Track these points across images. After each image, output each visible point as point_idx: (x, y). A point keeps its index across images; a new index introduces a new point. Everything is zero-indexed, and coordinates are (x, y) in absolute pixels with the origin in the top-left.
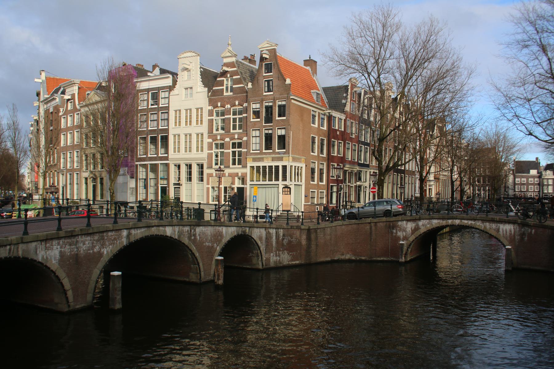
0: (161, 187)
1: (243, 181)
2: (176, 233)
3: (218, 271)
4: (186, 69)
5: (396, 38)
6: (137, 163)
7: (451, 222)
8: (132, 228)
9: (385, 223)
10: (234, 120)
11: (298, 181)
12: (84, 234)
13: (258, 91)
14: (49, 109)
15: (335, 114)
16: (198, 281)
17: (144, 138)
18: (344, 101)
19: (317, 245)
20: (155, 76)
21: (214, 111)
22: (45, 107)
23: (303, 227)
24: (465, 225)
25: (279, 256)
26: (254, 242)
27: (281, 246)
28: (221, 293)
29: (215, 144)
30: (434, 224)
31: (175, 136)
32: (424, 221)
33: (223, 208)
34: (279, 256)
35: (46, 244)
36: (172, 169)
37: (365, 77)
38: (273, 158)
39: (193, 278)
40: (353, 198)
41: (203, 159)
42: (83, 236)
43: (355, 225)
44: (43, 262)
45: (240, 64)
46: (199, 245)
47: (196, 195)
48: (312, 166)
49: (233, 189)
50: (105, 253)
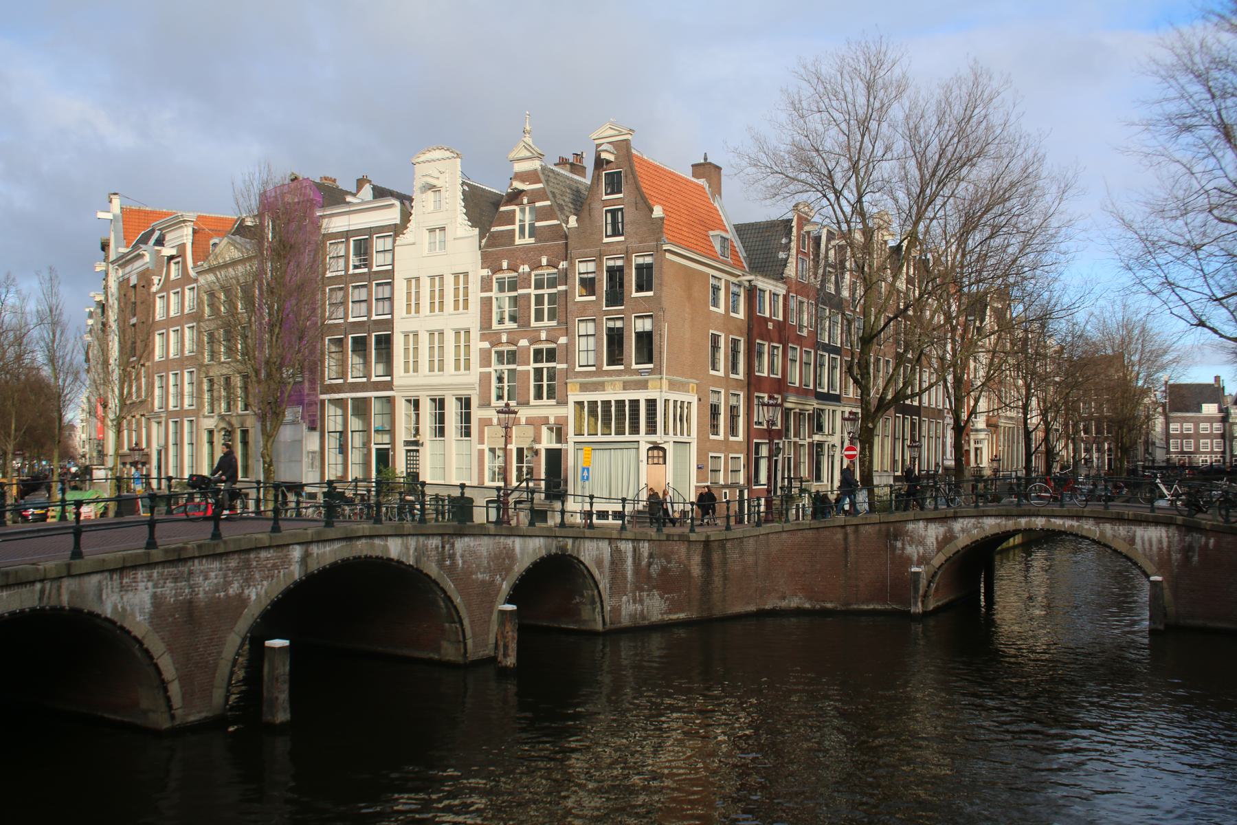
0: (377, 449)
1: (560, 434)
2: (411, 552)
3: (504, 637)
4: (432, 187)
5: (897, 112)
6: (323, 397)
7: (1026, 523)
8: (311, 542)
9: (877, 527)
10: (539, 299)
11: (682, 434)
12: (207, 556)
13: (592, 234)
14: (128, 280)
15: (762, 283)
16: (460, 659)
17: (340, 342)
18: (782, 255)
19: (725, 578)
20: (363, 202)
21: (494, 280)
22: (120, 273)
23: (693, 537)
24: (1057, 529)
25: (641, 602)
26: (586, 572)
27: (644, 580)
28: (512, 688)
29: (496, 352)
30: (987, 527)
31: (406, 336)
32: (966, 521)
33: (516, 495)
34: (641, 602)
35: (121, 578)
36: (402, 409)
37: (828, 200)
38: (624, 382)
39: (449, 652)
40: (804, 472)
41: (469, 386)
42: (204, 561)
43: (810, 532)
44: (116, 619)
45: (551, 175)
46: (463, 579)
47: (454, 466)
48: (713, 399)
49: (536, 453)
50: (253, 597)
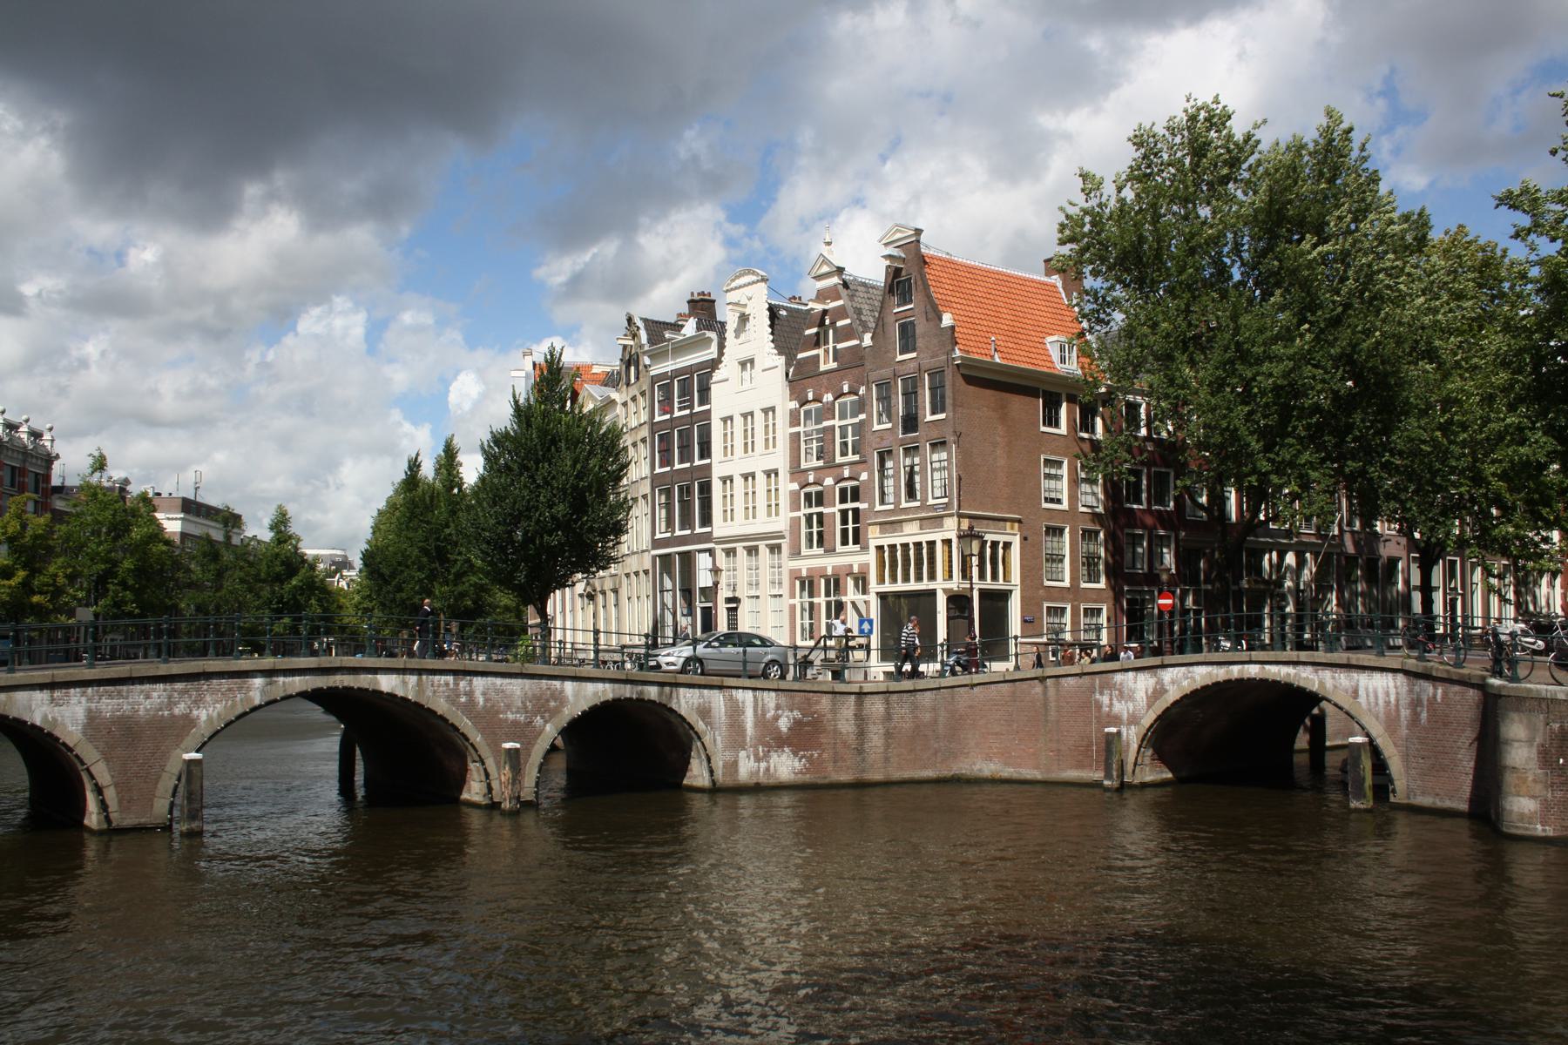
0: (702, 608)
1: (861, 581)
11: (995, 577)
24: (1271, 678)
30: (1198, 678)
45: (863, 289)
46: (488, 719)
